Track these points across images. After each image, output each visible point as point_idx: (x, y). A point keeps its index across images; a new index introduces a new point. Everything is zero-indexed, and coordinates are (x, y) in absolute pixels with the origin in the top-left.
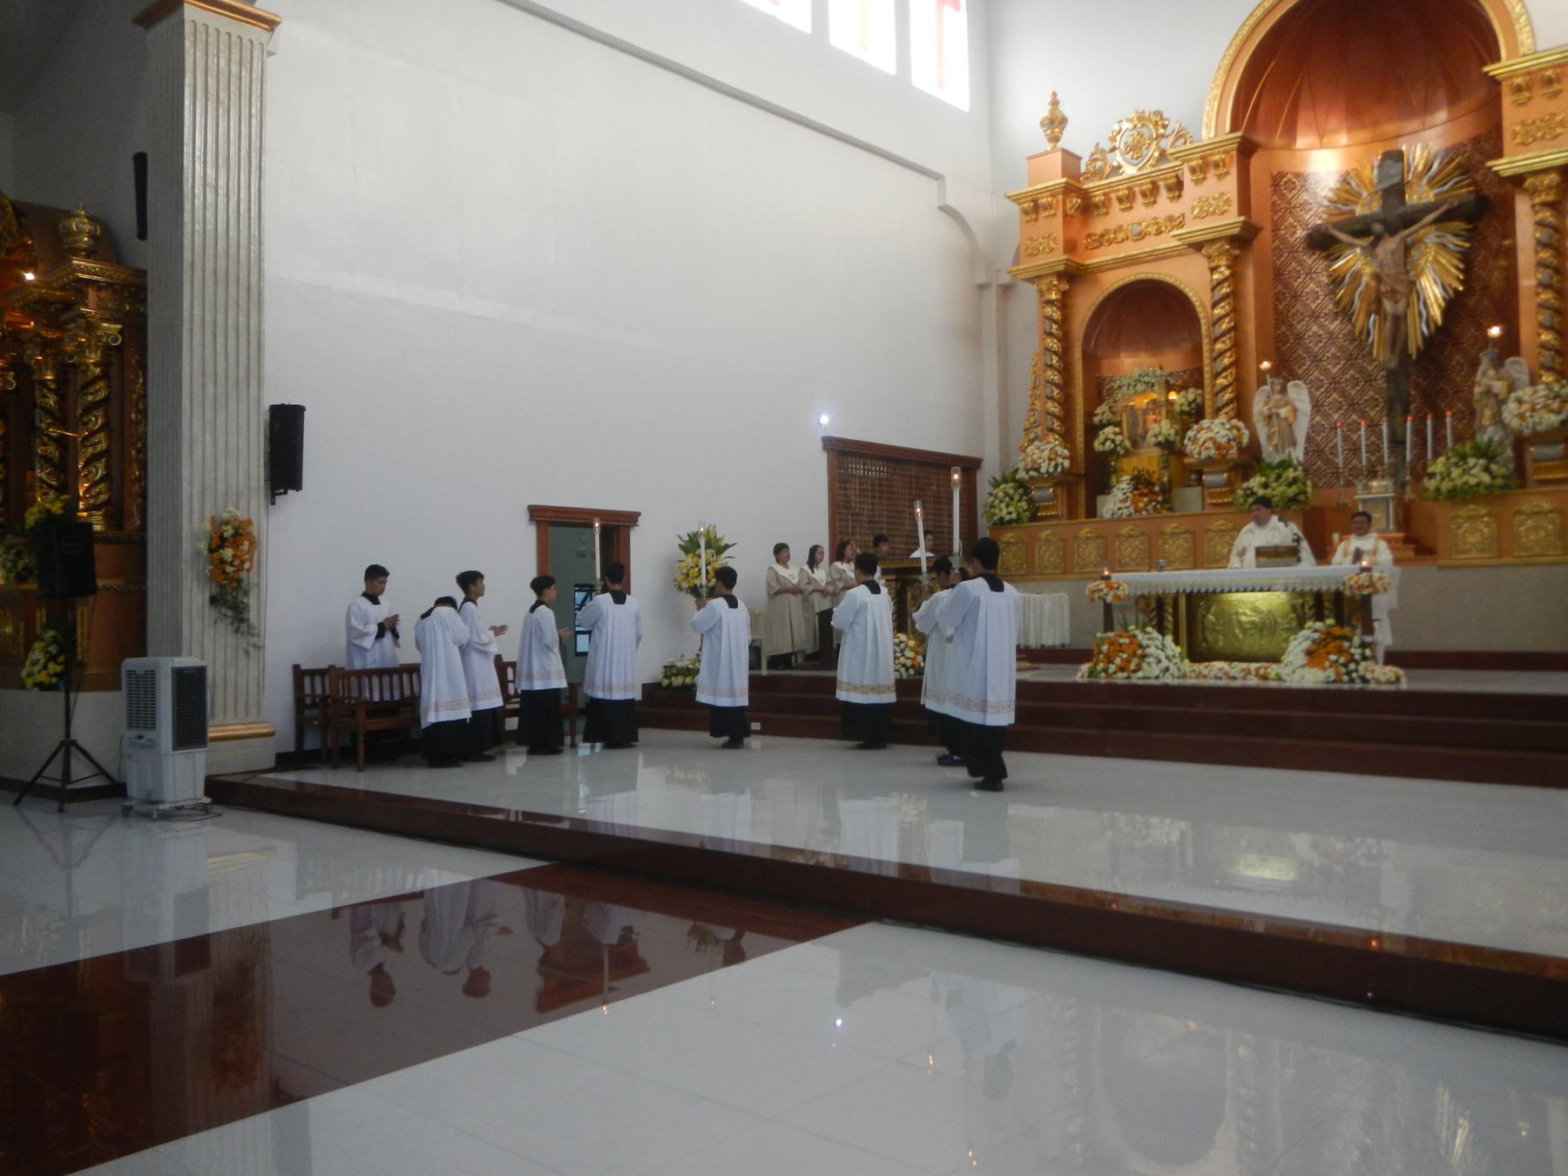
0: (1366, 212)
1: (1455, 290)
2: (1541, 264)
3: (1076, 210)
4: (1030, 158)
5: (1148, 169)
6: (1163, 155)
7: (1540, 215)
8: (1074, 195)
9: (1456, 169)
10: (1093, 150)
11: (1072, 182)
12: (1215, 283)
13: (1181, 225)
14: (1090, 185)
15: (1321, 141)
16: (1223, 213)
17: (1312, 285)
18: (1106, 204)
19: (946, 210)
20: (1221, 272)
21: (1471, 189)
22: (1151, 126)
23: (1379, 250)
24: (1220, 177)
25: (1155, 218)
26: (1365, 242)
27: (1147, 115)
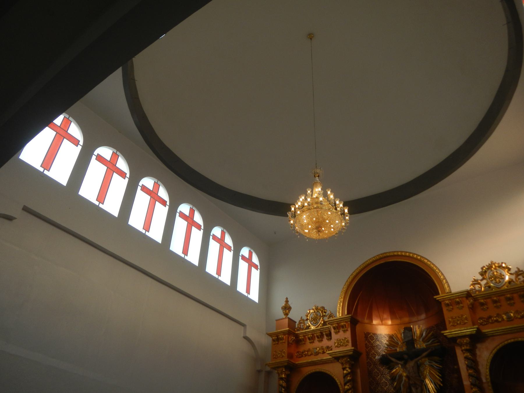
0: (401, 350)
1: (440, 385)
2: (470, 375)
3: (293, 341)
4: (277, 320)
5: (319, 328)
6: (325, 323)
7: (465, 355)
8: (292, 335)
9: (432, 335)
10: (300, 319)
11: (291, 330)
12: (345, 374)
13: (331, 350)
14: (299, 332)
15: (382, 322)
16: (346, 346)
17: (384, 379)
18: (304, 340)
19: (246, 338)
20: (347, 370)
21: (439, 344)
22: (320, 312)
23: (407, 366)
24: (344, 331)
25: (322, 347)
26: (402, 363)
27: (319, 308)
